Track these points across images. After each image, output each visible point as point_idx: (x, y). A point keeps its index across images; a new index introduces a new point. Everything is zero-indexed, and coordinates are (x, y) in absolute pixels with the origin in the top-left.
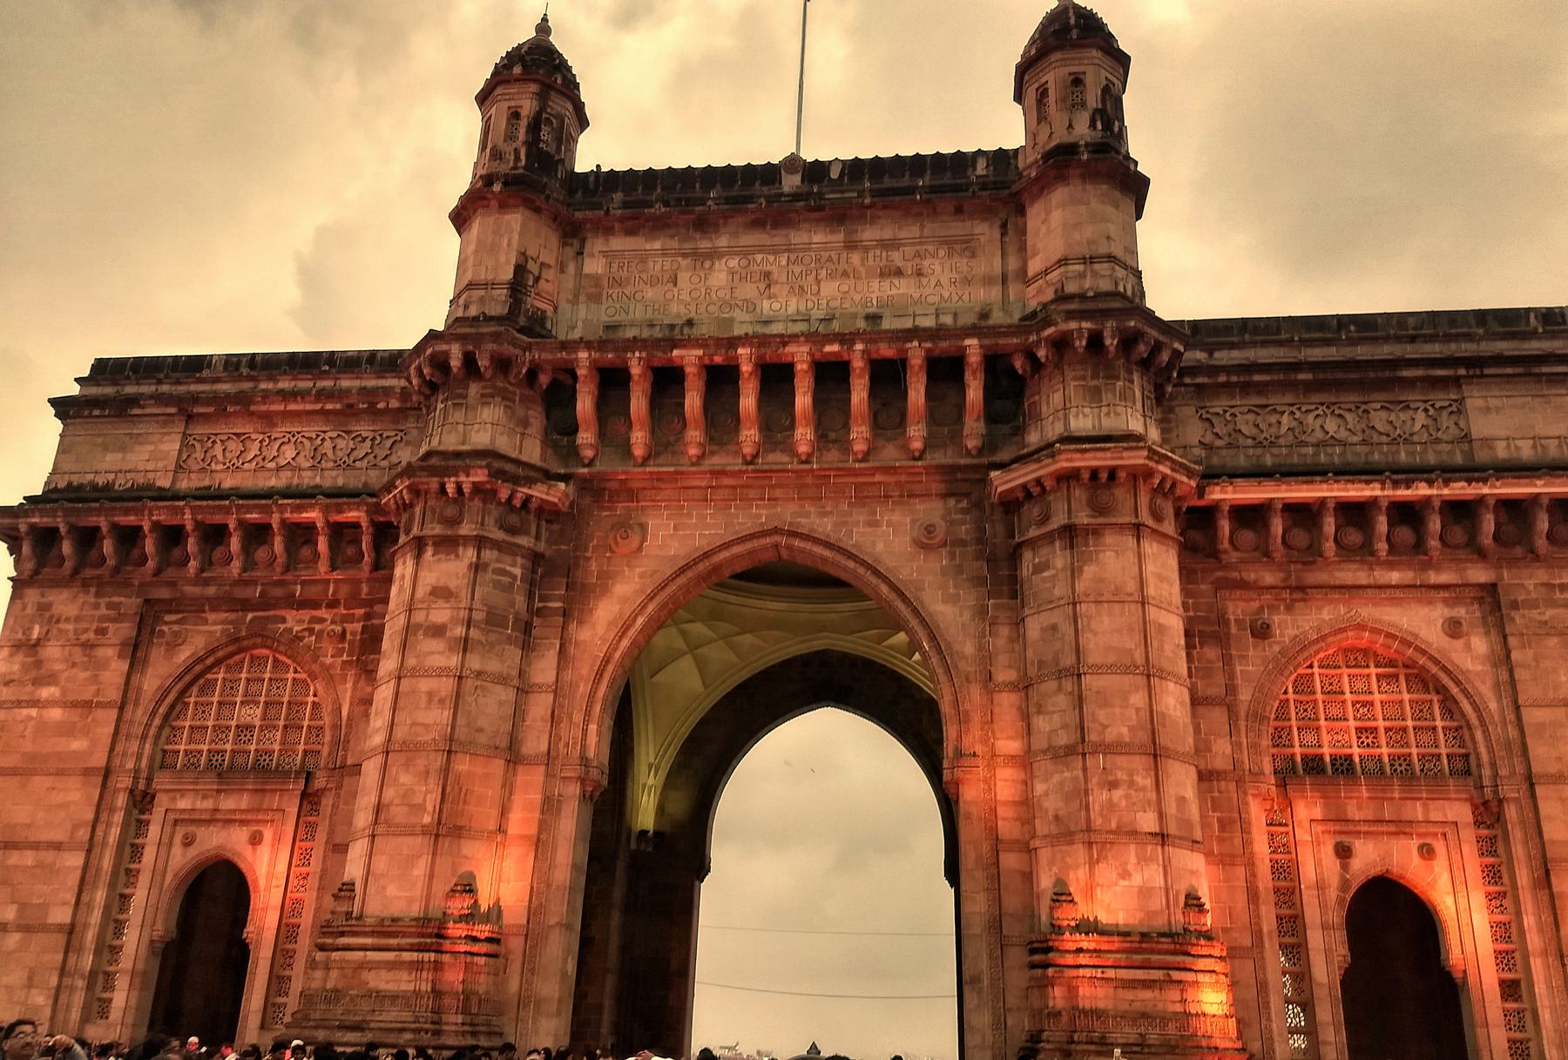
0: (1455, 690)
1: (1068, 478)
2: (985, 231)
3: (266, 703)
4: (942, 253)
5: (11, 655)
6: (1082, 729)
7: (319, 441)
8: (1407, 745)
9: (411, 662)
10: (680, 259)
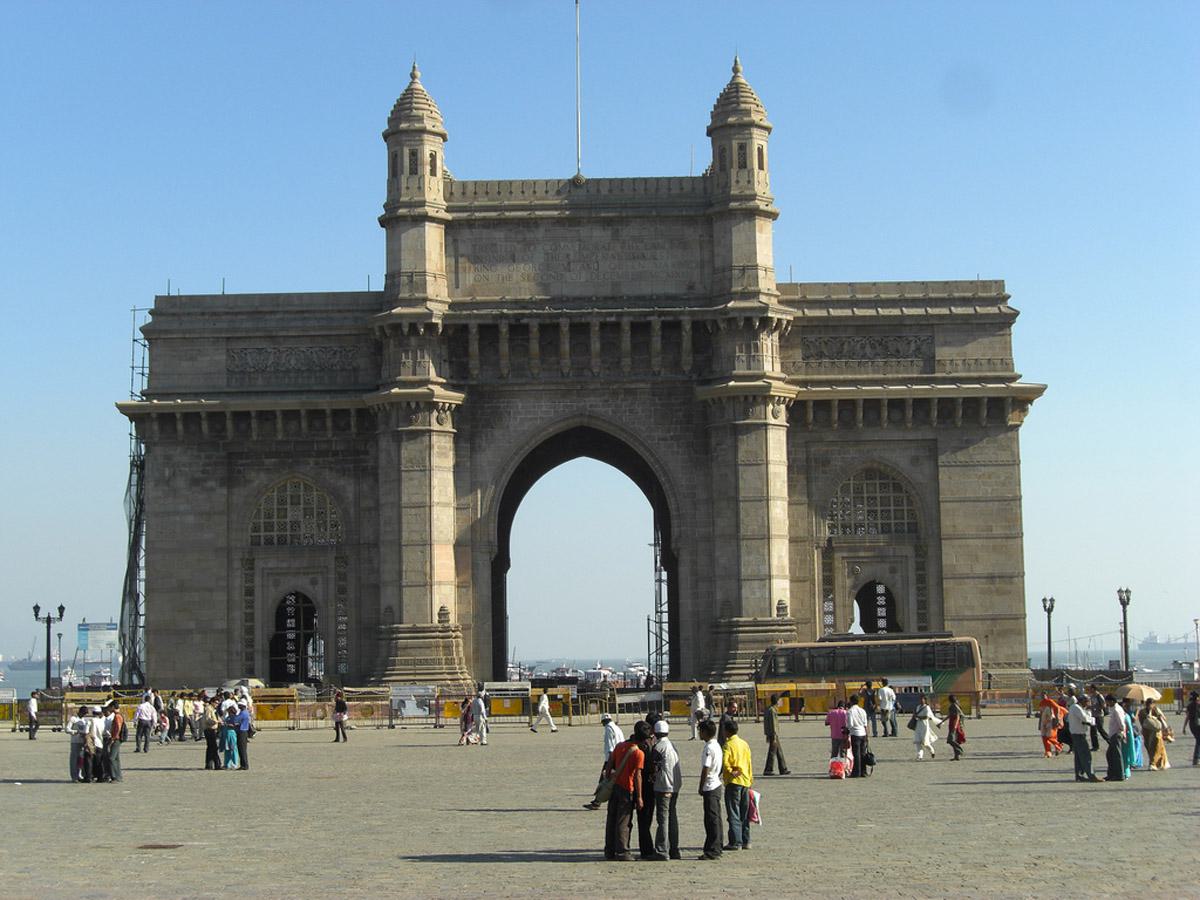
0: (913, 492)
1: (734, 398)
2: (692, 234)
3: (304, 509)
4: (667, 246)
5: (156, 485)
6: (738, 531)
7: (308, 353)
8: (890, 518)
9: (405, 499)
10: (515, 244)
